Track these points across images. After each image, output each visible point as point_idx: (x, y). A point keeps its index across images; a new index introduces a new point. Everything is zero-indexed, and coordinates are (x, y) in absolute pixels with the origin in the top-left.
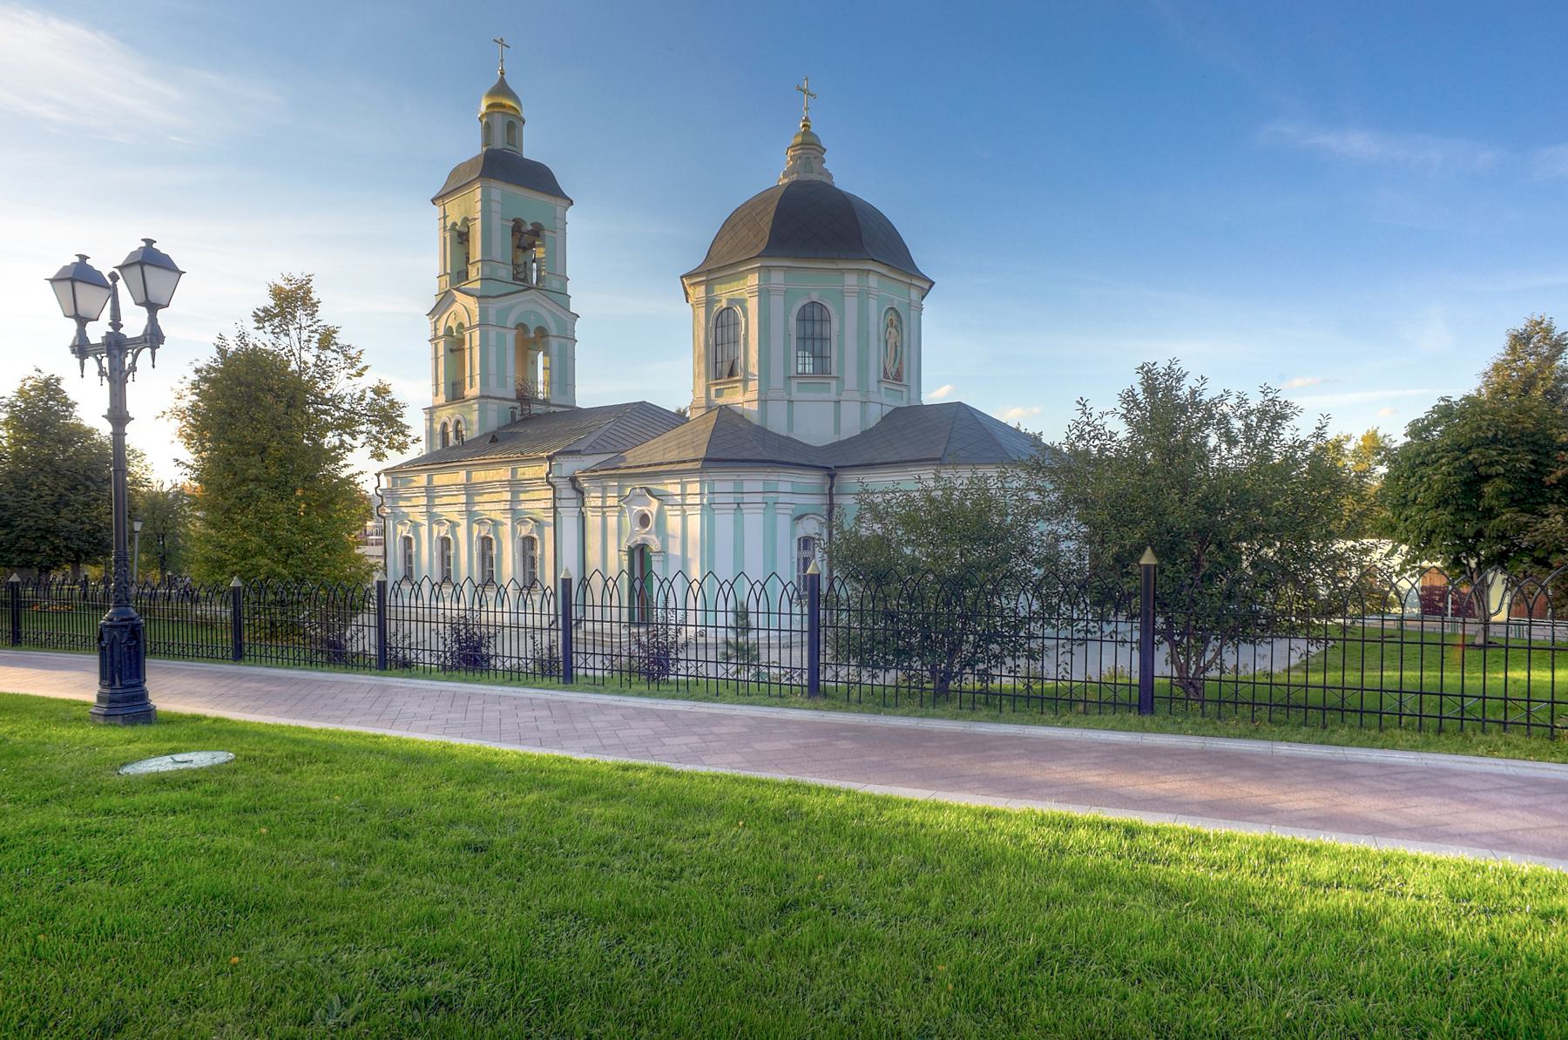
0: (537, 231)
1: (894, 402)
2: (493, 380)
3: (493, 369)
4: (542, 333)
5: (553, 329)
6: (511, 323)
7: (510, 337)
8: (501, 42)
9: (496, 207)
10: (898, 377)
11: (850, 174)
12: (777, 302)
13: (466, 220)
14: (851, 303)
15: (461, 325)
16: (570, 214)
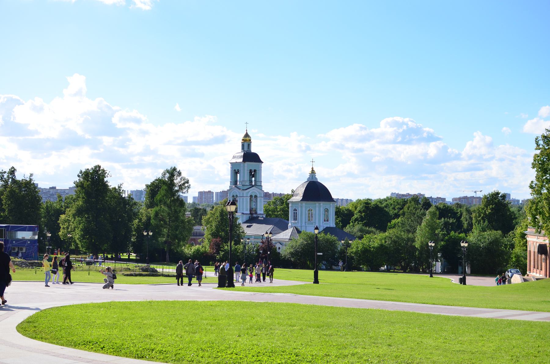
0: (255, 171)
1: (325, 226)
2: (245, 210)
3: (245, 207)
4: (256, 196)
5: (258, 196)
6: (249, 195)
7: (249, 198)
8: (247, 123)
9: (246, 168)
10: (328, 221)
11: (321, 178)
12: (304, 209)
13: (238, 170)
14: (317, 209)
15: (237, 196)
16: (263, 165)
